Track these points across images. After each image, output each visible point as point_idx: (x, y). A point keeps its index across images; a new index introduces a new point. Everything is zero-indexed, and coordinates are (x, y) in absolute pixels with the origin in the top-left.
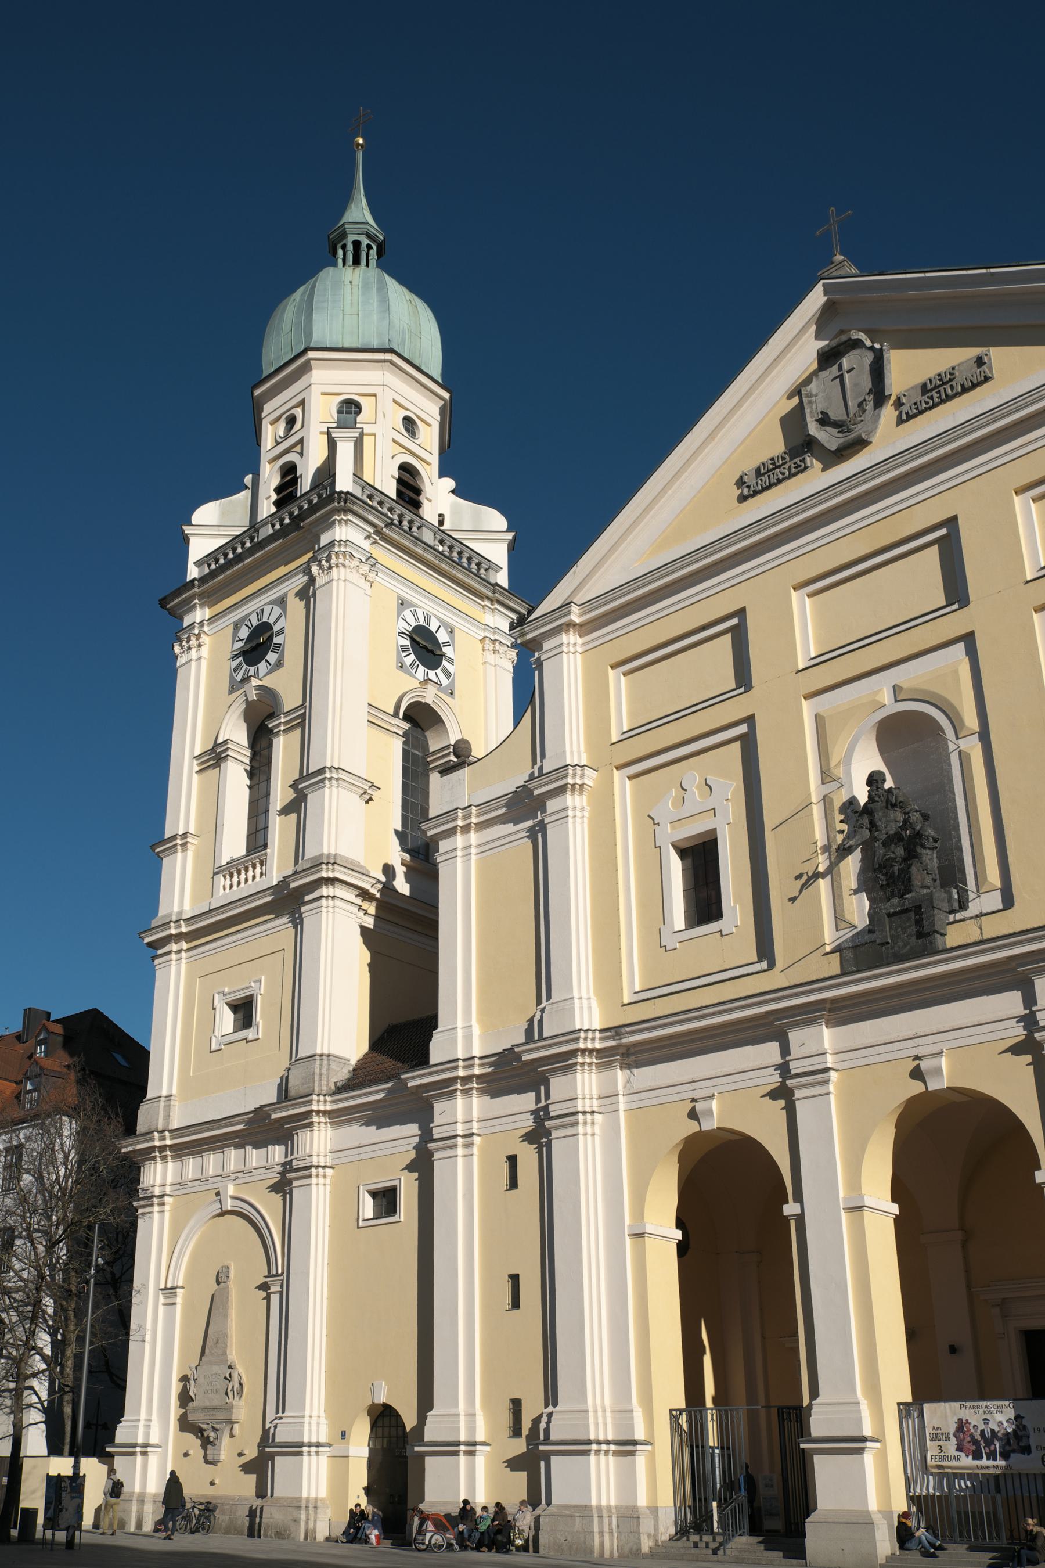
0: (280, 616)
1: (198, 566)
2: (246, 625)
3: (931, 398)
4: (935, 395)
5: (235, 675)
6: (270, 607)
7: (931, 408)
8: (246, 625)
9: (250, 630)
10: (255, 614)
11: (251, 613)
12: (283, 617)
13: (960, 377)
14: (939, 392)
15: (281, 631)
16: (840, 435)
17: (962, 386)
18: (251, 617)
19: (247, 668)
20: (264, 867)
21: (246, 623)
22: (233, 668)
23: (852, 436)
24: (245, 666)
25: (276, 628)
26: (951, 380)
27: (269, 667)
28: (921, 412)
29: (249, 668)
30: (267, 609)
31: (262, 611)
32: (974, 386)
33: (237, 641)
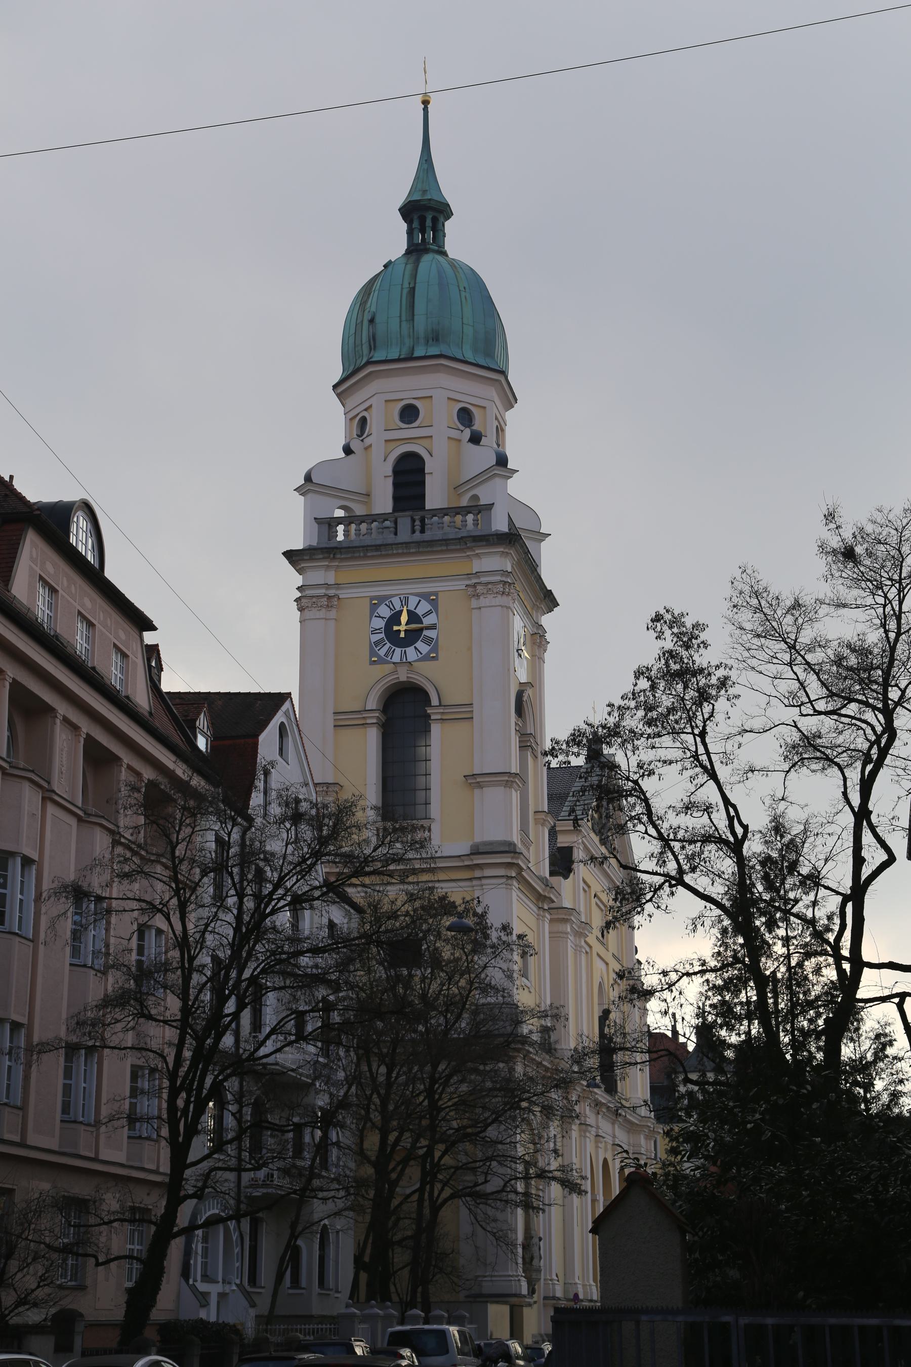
0: (429, 613)
1: (318, 523)
5: (377, 649)
6: (418, 599)
9: (392, 612)
10: (397, 598)
12: (434, 614)
15: (432, 627)
18: (393, 600)
19: (390, 648)
22: (373, 641)
24: (388, 645)
29: (394, 648)
30: (413, 601)
31: (407, 599)
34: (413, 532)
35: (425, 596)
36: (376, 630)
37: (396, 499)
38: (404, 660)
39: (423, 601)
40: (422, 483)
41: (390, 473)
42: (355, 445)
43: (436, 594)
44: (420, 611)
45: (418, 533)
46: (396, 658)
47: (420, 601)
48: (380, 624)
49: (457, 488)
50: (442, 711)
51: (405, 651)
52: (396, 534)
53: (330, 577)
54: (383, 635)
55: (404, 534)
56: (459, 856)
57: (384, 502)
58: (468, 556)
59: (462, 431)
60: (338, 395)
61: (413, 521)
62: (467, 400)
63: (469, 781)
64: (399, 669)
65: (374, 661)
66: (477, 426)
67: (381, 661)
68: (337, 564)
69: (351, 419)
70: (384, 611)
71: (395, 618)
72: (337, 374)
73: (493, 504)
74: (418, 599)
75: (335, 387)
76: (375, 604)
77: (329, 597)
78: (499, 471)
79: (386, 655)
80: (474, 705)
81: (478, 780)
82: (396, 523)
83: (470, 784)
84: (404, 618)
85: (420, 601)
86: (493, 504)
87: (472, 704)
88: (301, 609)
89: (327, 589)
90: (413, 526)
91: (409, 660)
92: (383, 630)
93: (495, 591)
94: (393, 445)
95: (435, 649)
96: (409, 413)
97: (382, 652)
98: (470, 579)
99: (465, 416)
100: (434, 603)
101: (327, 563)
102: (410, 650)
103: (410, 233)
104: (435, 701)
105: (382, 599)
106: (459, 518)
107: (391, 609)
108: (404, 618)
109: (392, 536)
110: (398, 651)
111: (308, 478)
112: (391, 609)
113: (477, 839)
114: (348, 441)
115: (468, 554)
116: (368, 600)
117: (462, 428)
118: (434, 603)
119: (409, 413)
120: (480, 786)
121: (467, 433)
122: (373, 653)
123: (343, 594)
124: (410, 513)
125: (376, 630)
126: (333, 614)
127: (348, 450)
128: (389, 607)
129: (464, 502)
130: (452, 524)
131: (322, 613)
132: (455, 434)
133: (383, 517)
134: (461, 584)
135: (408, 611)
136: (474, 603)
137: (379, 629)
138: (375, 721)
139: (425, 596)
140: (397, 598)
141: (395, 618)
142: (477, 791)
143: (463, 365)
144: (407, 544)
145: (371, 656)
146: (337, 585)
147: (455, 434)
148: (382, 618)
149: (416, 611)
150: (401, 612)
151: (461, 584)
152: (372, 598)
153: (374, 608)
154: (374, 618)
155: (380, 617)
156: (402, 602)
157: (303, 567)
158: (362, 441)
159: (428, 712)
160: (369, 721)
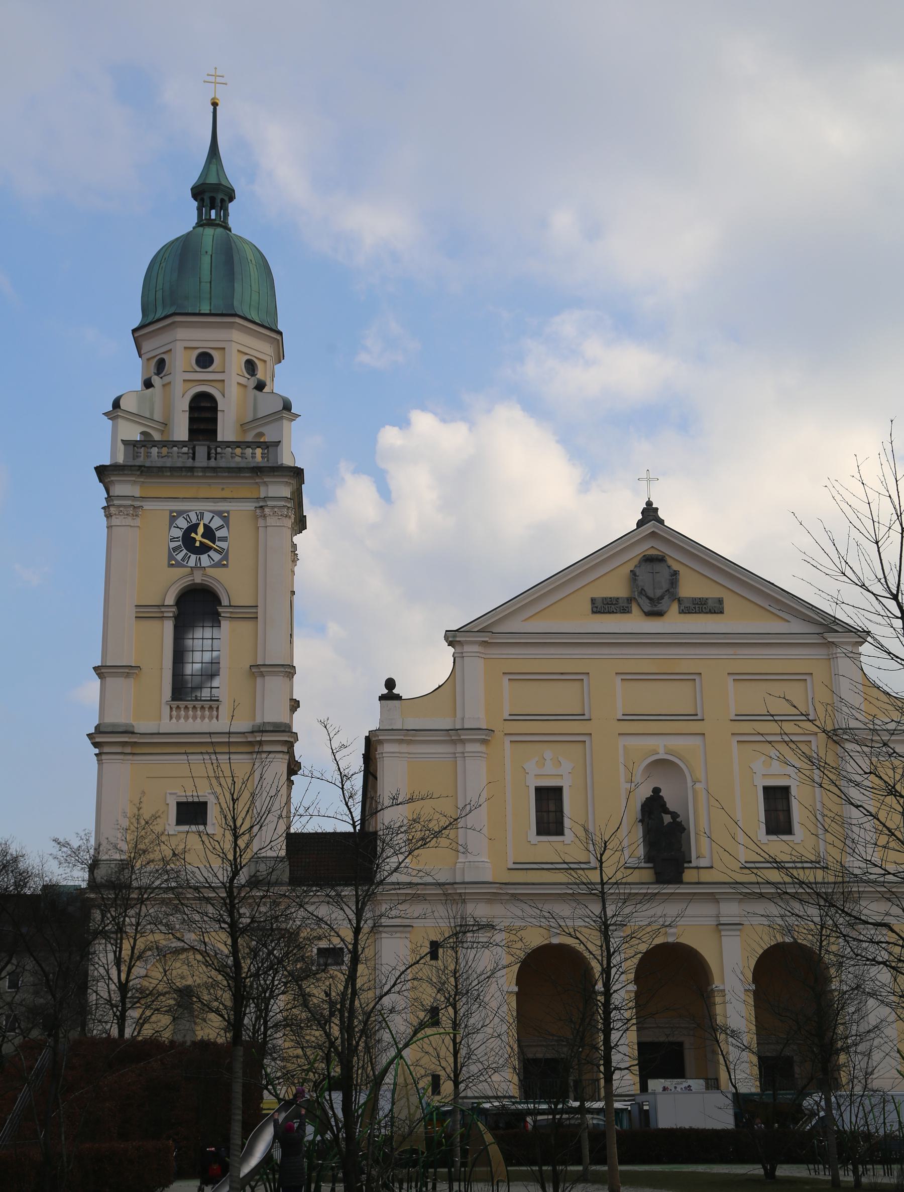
0: (221, 527)
2: (184, 517)
3: (695, 608)
4: (697, 609)
5: (174, 554)
6: (212, 515)
7: (693, 613)
8: (184, 517)
9: (189, 525)
10: (194, 512)
11: (193, 510)
13: (710, 603)
14: (699, 607)
15: (224, 539)
16: (649, 604)
17: (710, 610)
20: (215, 713)
21: (185, 516)
23: (656, 609)
24: (185, 551)
25: (218, 534)
26: (705, 604)
27: (212, 562)
28: (689, 613)
29: (190, 554)
30: (207, 517)
31: (202, 514)
32: (715, 613)
33: (174, 527)
34: (209, 458)
35: (219, 514)
36: (175, 538)
37: (191, 431)
38: (199, 565)
39: (216, 517)
40: (215, 420)
41: (187, 409)
42: (156, 380)
43: (228, 512)
44: (213, 525)
45: (213, 460)
46: (192, 562)
47: (213, 516)
48: (179, 533)
49: (244, 427)
50: (231, 610)
51: (200, 557)
52: (194, 458)
53: (135, 491)
54: (180, 543)
55: (201, 460)
56: (244, 733)
57: (181, 431)
58: (257, 483)
59: (248, 379)
60: (136, 340)
61: (209, 449)
62: (254, 354)
63: (253, 670)
64: (195, 572)
65: (173, 564)
66: (260, 375)
67: (178, 565)
68: (142, 480)
69: (148, 360)
70: (183, 523)
71: (193, 528)
72: (136, 319)
73: (280, 442)
74: (212, 515)
75: (134, 331)
76: (174, 516)
77: (135, 507)
78: (285, 414)
79: (183, 559)
80: (259, 608)
81: (262, 670)
82: (194, 449)
83: (253, 673)
84: (201, 530)
85: (213, 516)
86: (280, 442)
87: (257, 606)
88: (108, 516)
89: (133, 501)
90: (209, 454)
91: (202, 566)
92: (181, 538)
93: (280, 514)
94: (190, 385)
95: (226, 558)
96: (204, 360)
97: (179, 557)
98: (258, 502)
99: (251, 366)
100: (226, 519)
101: (134, 479)
102: (204, 558)
103: (199, 209)
104: (225, 602)
105: (180, 513)
106: (249, 451)
107: (188, 522)
108: (201, 530)
109: (190, 460)
110: (193, 557)
111: (116, 404)
112: (188, 522)
113: (259, 720)
114: (146, 377)
115: (257, 481)
116: (168, 511)
117: (249, 377)
118: (226, 519)
119: (204, 360)
120: (262, 675)
121: (252, 383)
122: (171, 557)
123: (147, 506)
124: (207, 443)
125: (175, 538)
126: (138, 522)
127: (148, 384)
128: (186, 519)
129: (249, 438)
130: (233, 455)
131: (129, 521)
132: (243, 381)
133: (183, 444)
134: (250, 506)
135: (204, 524)
136: (261, 522)
137: (177, 538)
138: (171, 615)
139: (219, 514)
140: (194, 512)
141: (193, 528)
142: (259, 680)
143: (251, 324)
144: (205, 469)
145: (169, 562)
146: (143, 498)
147: (243, 381)
148: (180, 528)
149: (210, 525)
150: (197, 525)
151: (250, 506)
152: (171, 512)
153: (173, 519)
154: (173, 529)
155: (178, 527)
156: (197, 516)
157: (112, 481)
158: (161, 378)
159: (220, 610)
160: (166, 615)
